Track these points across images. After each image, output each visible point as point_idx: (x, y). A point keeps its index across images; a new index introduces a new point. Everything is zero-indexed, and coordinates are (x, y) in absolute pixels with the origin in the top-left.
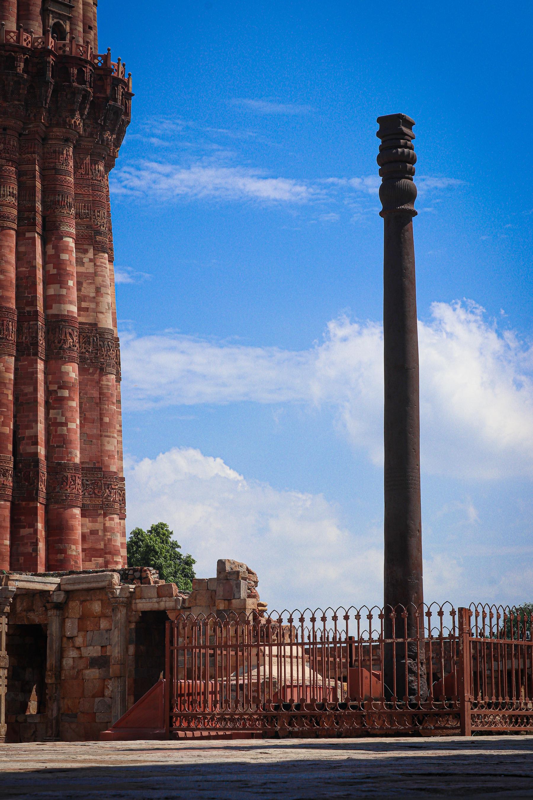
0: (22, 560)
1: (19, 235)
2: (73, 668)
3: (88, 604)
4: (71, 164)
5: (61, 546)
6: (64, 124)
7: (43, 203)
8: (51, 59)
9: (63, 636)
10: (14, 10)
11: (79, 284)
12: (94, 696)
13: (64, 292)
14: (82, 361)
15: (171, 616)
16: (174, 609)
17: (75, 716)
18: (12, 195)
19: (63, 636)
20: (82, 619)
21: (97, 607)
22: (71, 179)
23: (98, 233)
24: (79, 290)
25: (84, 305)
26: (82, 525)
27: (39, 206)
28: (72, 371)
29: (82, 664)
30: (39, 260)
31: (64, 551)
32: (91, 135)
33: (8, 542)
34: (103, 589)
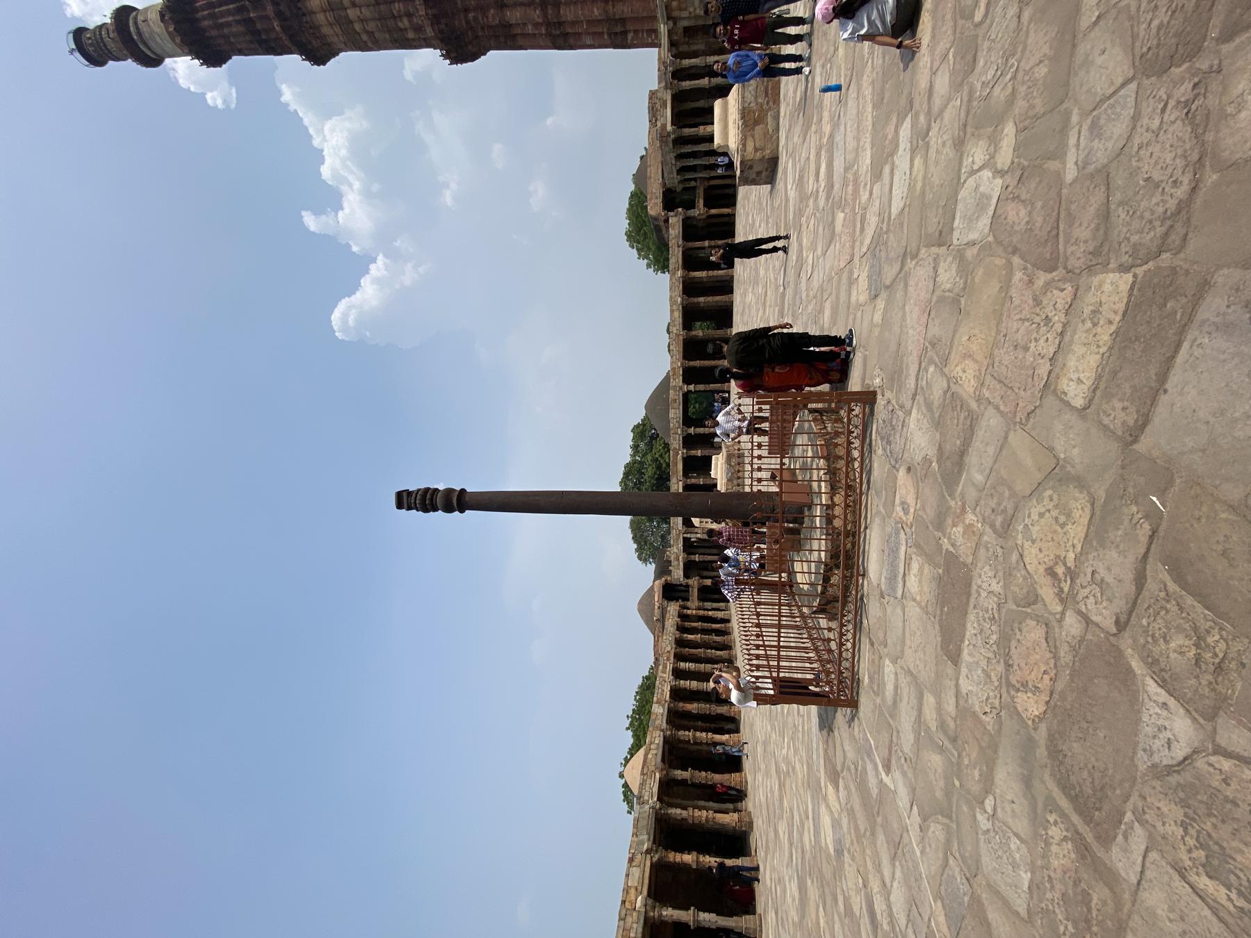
9: (689, 18)
19: (689, 18)
20: (681, 9)
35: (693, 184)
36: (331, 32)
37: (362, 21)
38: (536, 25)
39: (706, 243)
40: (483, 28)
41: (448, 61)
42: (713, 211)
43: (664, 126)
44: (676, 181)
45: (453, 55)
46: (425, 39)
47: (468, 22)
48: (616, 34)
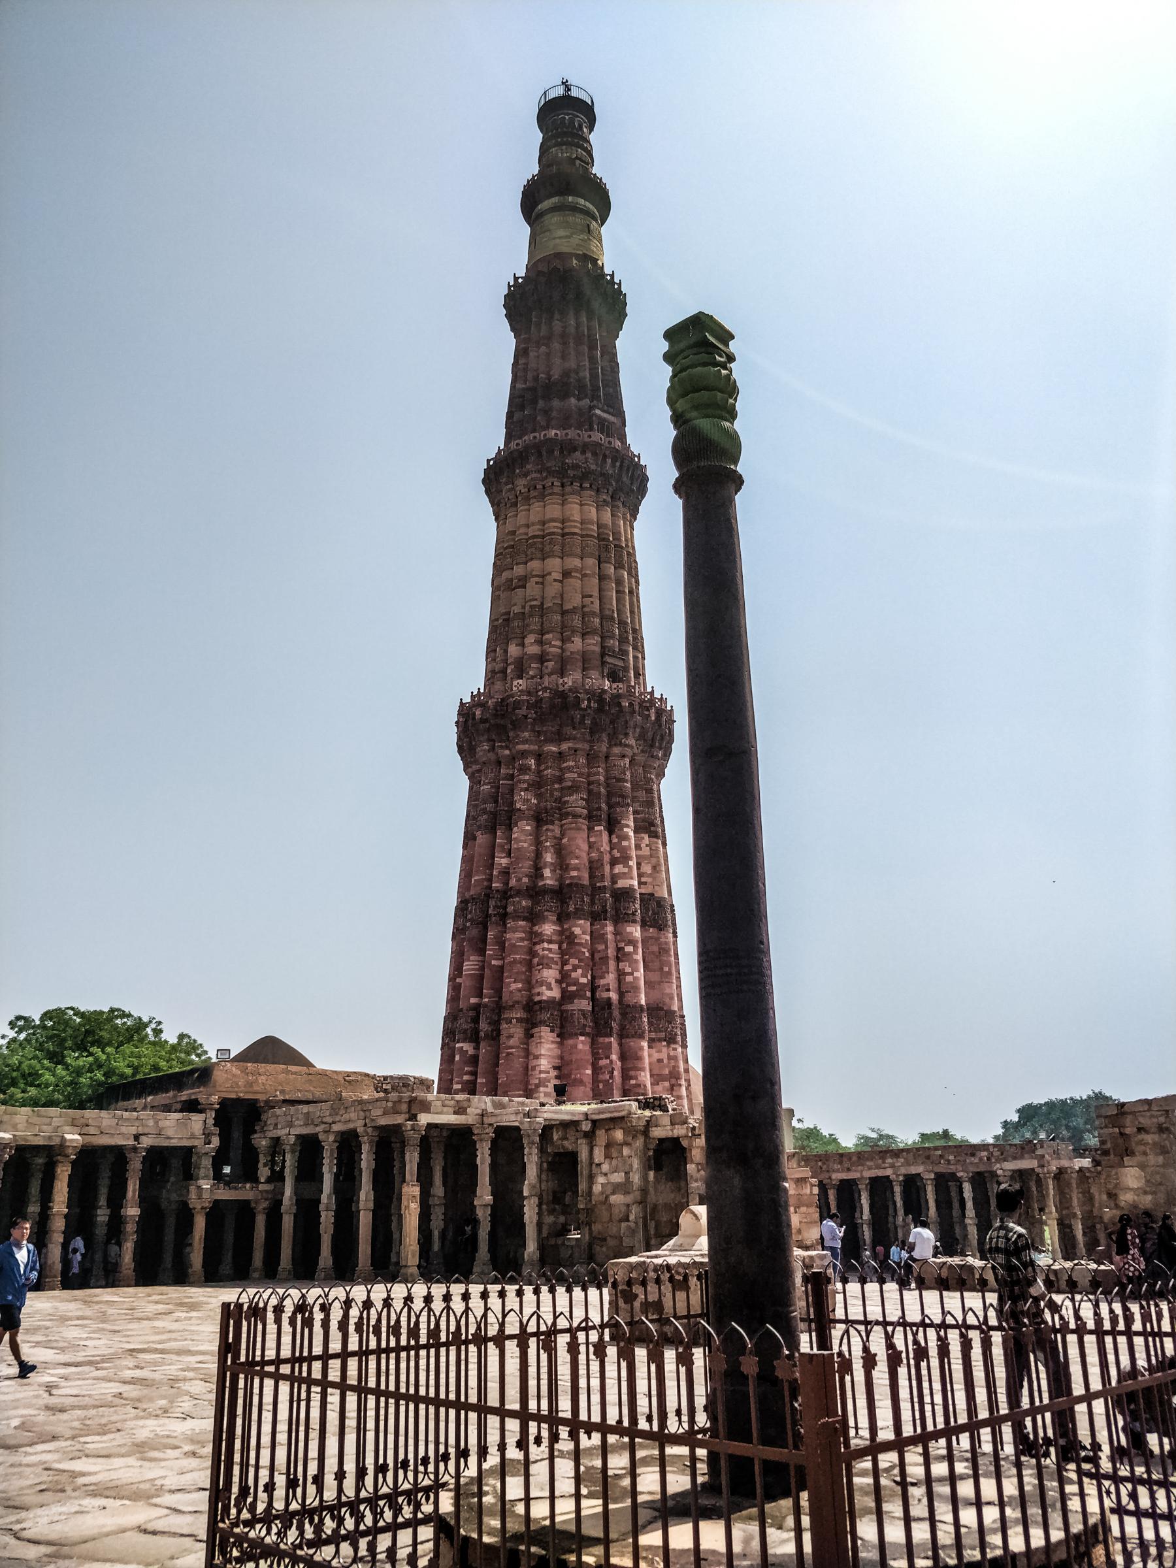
0: (601, 1086)
1: (590, 829)
2: (602, 1193)
3: (611, 1132)
4: (628, 773)
5: (632, 1073)
6: (621, 744)
7: (608, 804)
8: (607, 697)
10: (580, 664)
11: (639, 864)
12: (620, 1221)
13: (626, 870)
14: (644, 925)
15: (685, 1143)
16: (687, 1136)
17: (605, 1240)
18: (582, 799)
19: (591, 1163)
20: (608, 1146)
21: (619, 1135)
22: (629, 785)
23: (652, 824)
24: (638, 869)
25: (643, 880)
26: (650, 1056)
27: (603, 806)
28: (636, 931)
29: (609, 1190)
30: (605, 847)
31: (636, 1078)
32: (642, 751)
33: (589, 1072)
34: (623, 1118)
35: (264, 1172)
36: (534, 518)
37: (543, 576)
38: (506, 873)
39: (132, 1211)
40: (512, 777)
41: (467, 699)
42: (200, 1223)
43: (426, 1107)
44: (281, 1132)
45: (478, 712)
46: (504, 671)
47: (524, 754)
48: (476, 1020)
